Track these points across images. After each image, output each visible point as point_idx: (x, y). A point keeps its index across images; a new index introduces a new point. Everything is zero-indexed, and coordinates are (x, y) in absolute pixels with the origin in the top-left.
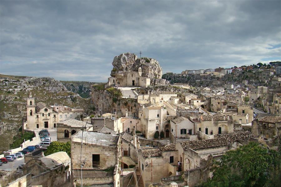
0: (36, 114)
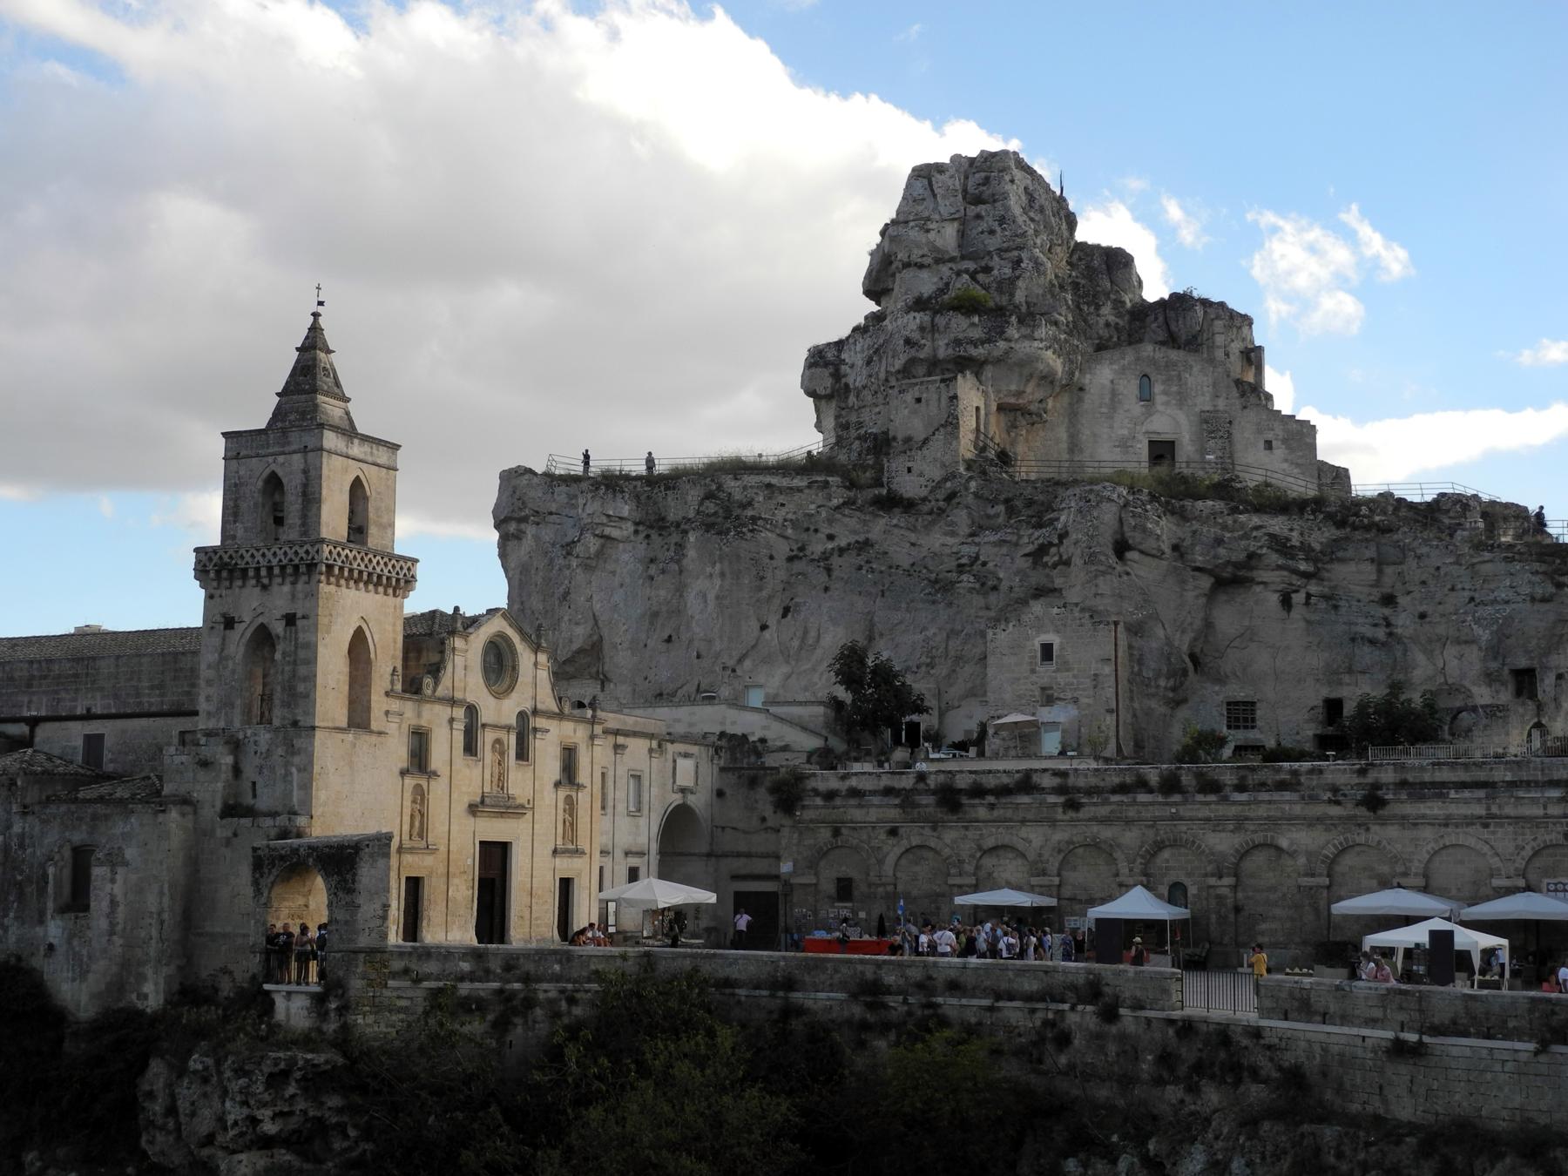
0: (408, 708)
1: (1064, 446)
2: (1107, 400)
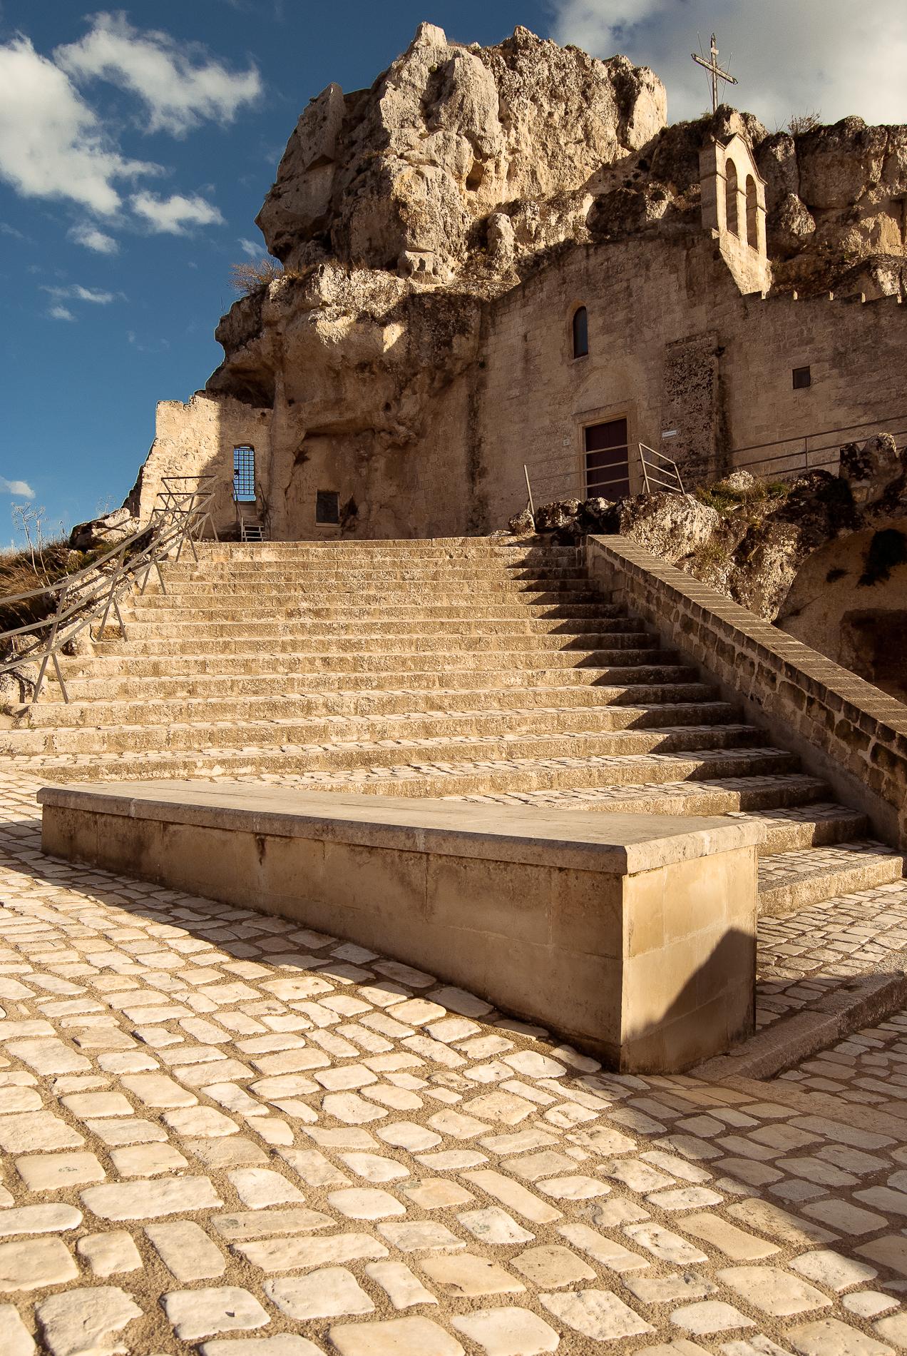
1: (462, 470)
2: (518, 374)
